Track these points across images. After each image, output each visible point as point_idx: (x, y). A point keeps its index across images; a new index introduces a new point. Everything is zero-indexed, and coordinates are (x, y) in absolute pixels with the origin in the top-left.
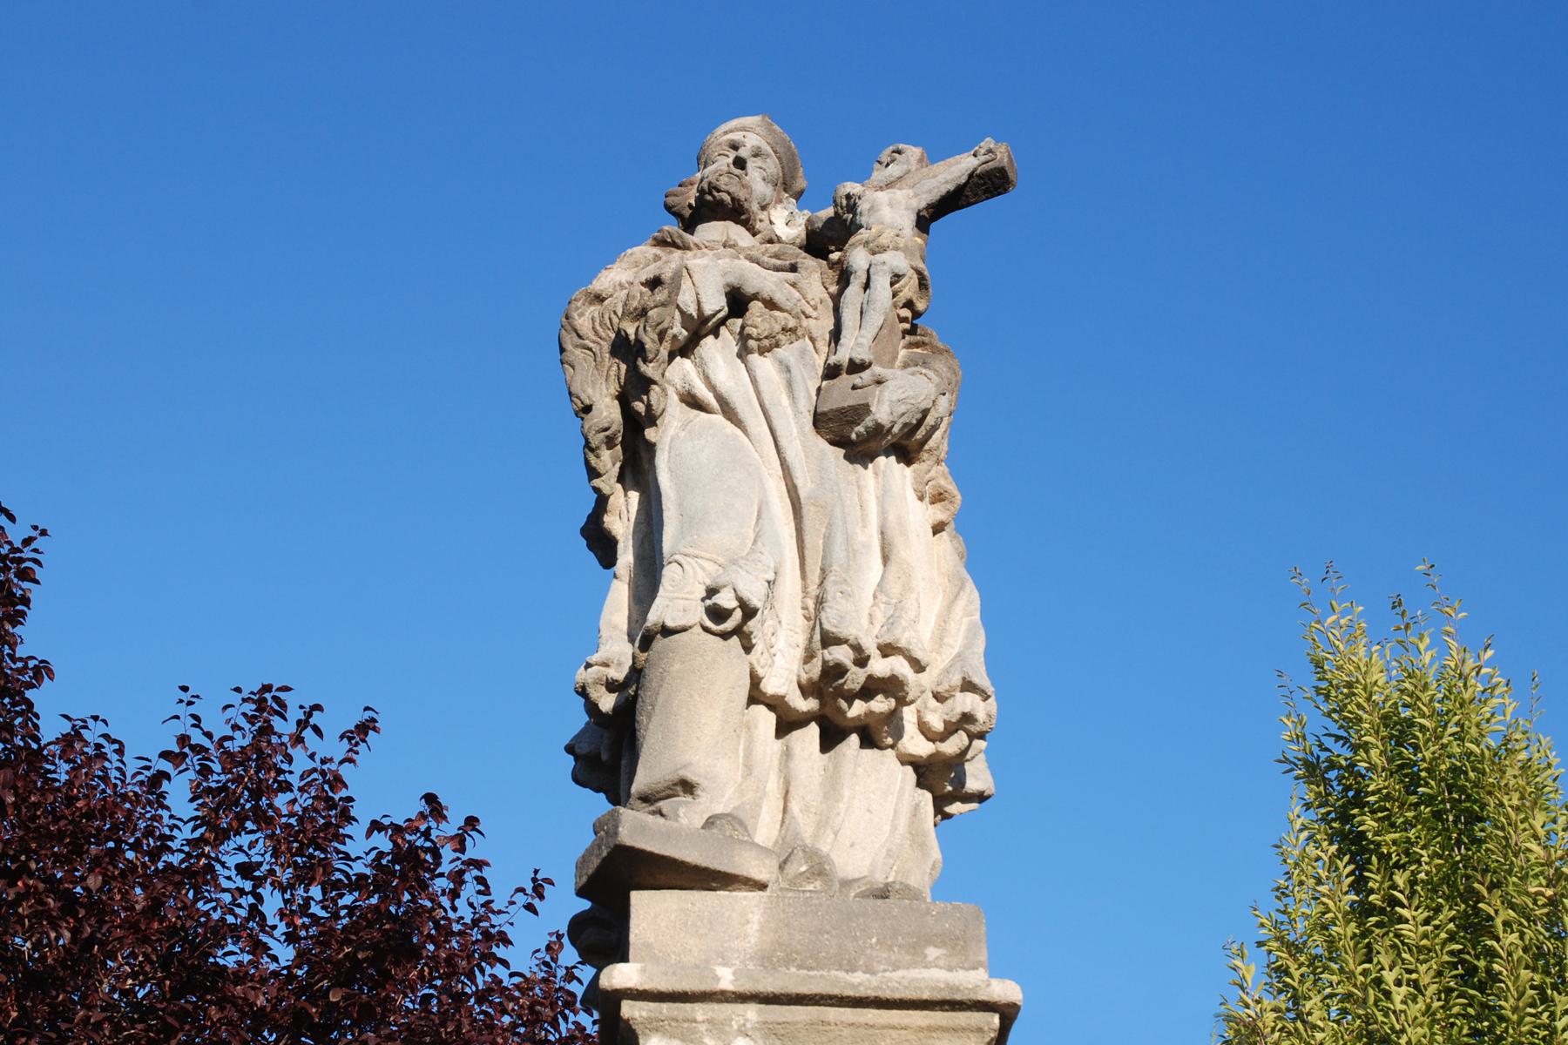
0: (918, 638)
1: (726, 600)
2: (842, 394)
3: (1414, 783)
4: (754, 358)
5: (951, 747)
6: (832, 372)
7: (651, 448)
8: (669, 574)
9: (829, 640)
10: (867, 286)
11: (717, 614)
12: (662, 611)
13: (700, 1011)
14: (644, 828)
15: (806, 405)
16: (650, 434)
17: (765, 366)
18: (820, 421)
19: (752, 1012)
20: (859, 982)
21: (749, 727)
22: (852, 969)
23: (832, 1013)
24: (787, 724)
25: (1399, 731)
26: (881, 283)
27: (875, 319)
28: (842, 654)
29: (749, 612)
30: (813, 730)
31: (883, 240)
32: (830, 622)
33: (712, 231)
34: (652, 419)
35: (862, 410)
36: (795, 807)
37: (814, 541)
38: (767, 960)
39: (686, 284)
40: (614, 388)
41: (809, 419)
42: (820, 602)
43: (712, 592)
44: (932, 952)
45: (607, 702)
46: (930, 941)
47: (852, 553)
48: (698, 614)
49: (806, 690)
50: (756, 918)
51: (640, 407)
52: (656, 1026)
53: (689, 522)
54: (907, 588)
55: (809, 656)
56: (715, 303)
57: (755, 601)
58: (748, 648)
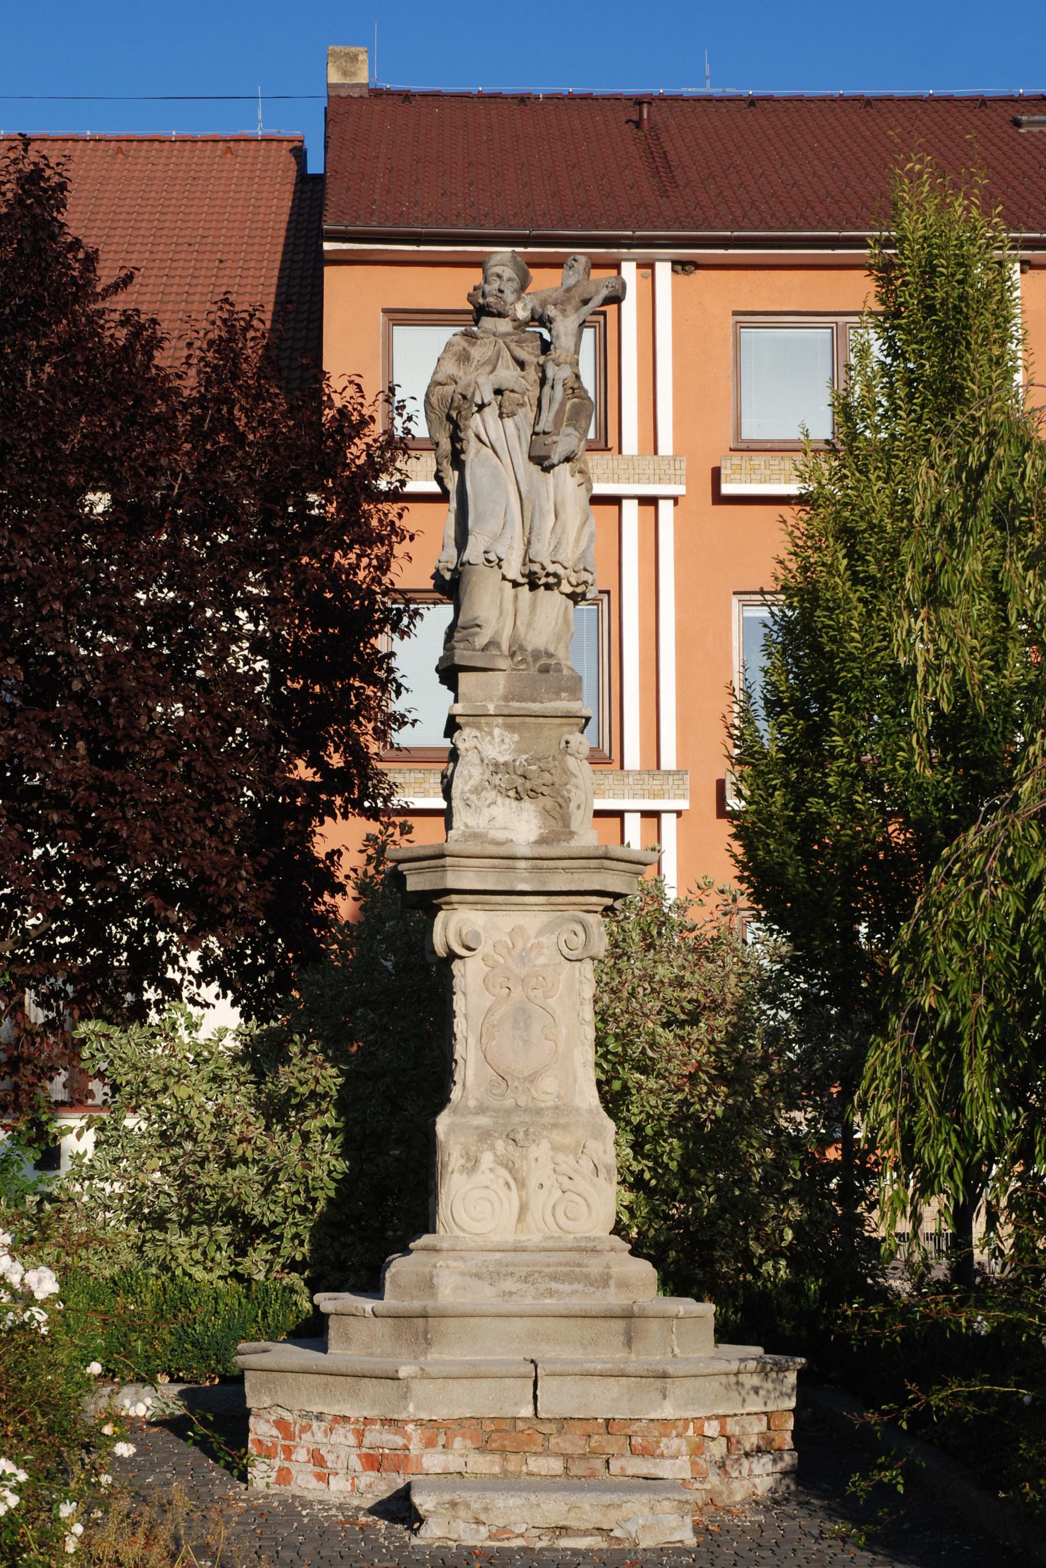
0: (568, 554)
1: (492, 557)
2: (538, 452)
3: (931, 310)
4: (506, 420)
5: (579, 590)
6: (535, 433)
7: (464, 462)
8: (471, 538)
9: (531, 561)
10: (553, 387)
11: (489, 561)
12: (468, 555)
13: (483, 720)
14: (462, 657)
15: (526, 449)
16: (463, 457)
17: (509, 422)
18: (531, 458)
19: (500, 720)
20: (536, 707)
21: (501, 590)
22: (535, 701)
23: (528, 719)
24: (516, 584)
25: (930, 271)
26: (559, 389)
27: (556, 406)
28: (536, 568)
29: (500, 560)
30: (527, 587)
31: (561, 360)
32: (532, 554)
33: (487, 322)
34: (463, 452)
35: (548, 457)
36: (518, 622)
37: (528, 514)
38: (506, 699)
39: (477, 393)
40: (448, 434)
41: (526, 456)
42: (529, 542)
43: (486, 552)
44: (563, 695)
45: (448, 576)
46: (563, 690)
47: (542, 515)
48: (481, 560)
49: (523, 576)
50: (502, 683)
51: (458, 446)
52: (467, 724)
53: (479, 518)
54: (563, 532)
55: (524, 564)
56: (489, 396)
57: (503, 557)
58: (500, 567)
